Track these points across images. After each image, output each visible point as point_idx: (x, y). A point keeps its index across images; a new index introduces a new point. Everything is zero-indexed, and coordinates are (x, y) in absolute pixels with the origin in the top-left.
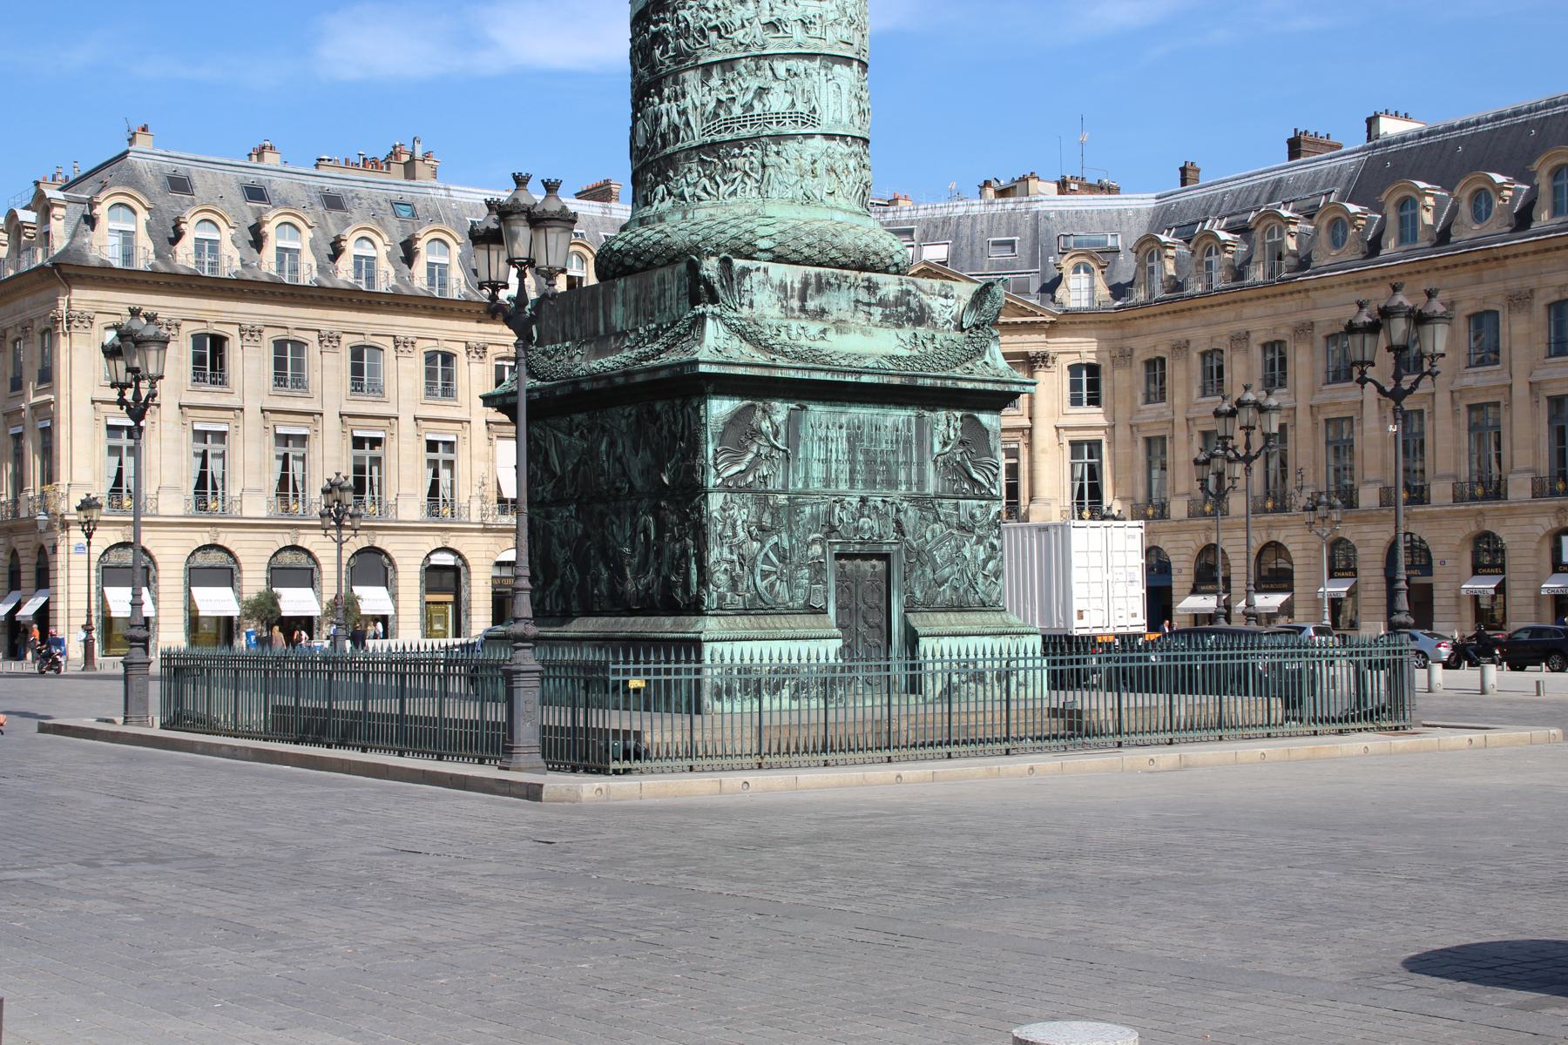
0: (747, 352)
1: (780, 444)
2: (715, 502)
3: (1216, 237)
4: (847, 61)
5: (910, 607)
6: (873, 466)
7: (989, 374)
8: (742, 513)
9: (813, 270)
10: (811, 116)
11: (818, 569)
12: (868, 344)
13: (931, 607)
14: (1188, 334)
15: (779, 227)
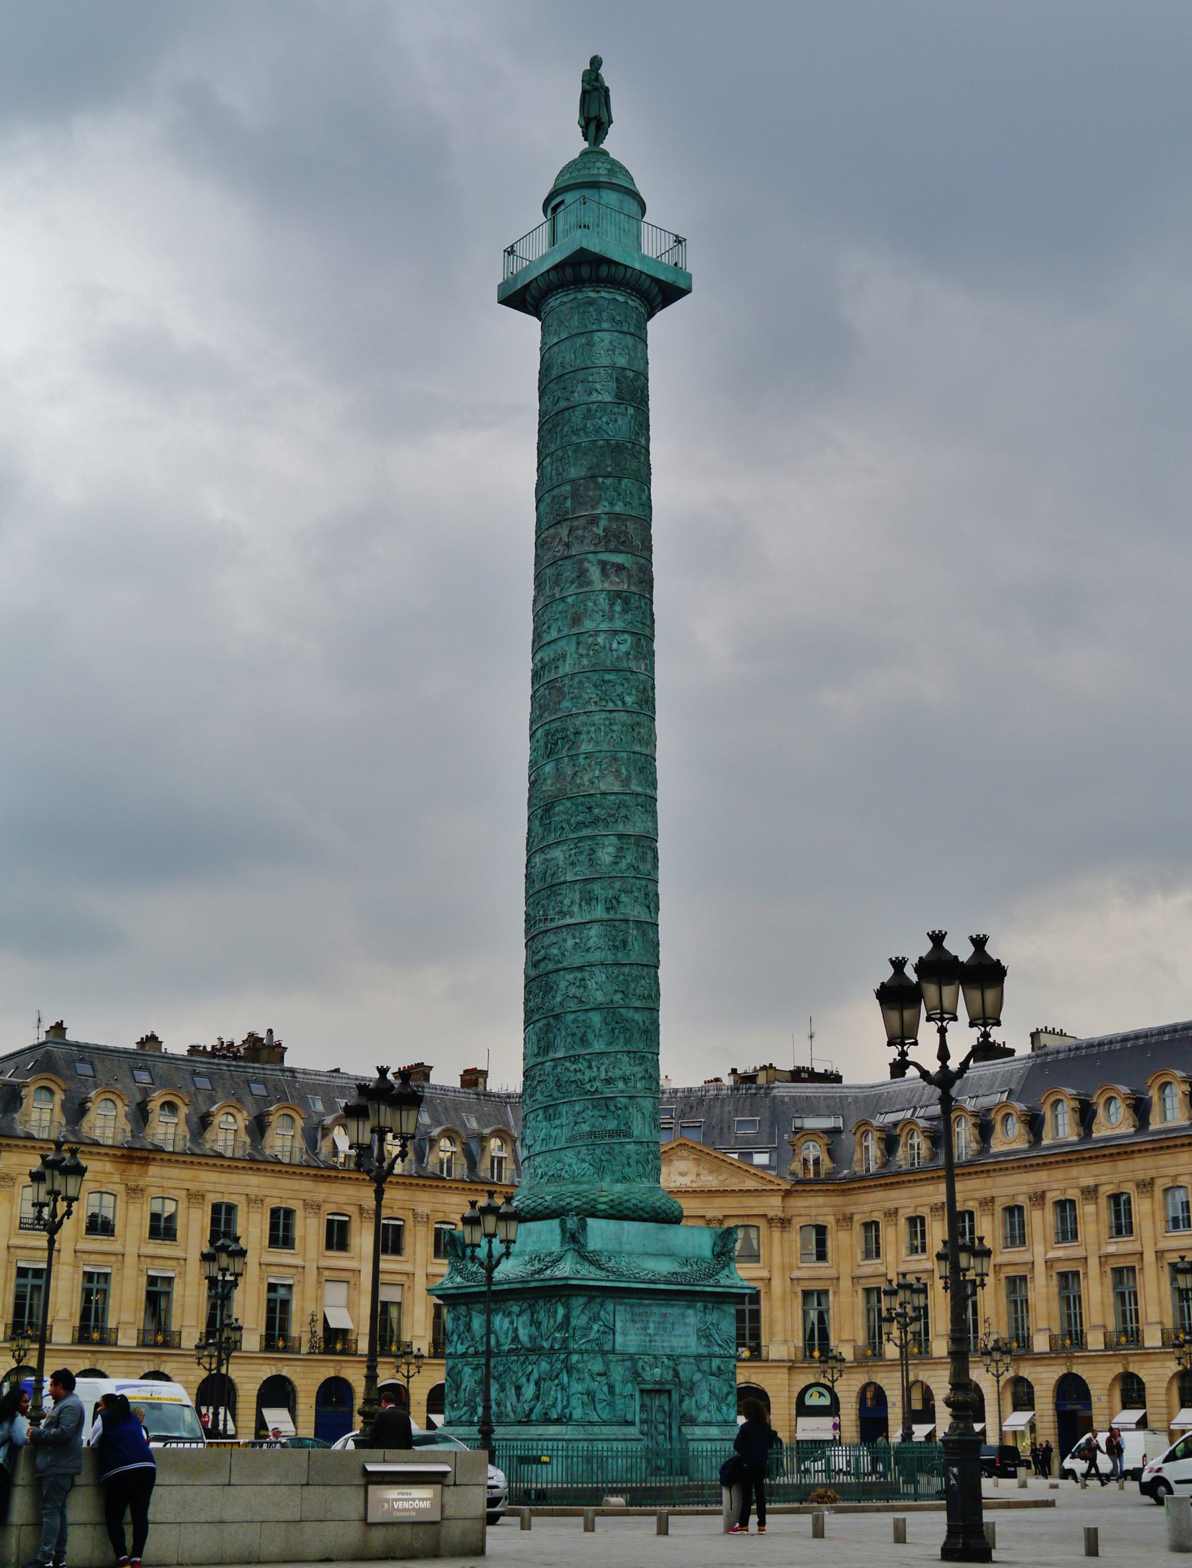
15: (611, 1197)
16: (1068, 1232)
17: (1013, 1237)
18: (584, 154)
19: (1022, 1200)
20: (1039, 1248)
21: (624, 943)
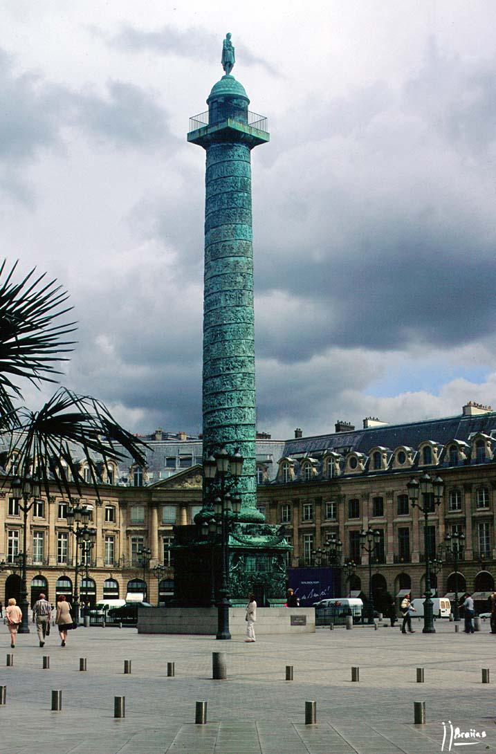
0: (237, 543)
1: (242, 562)
2: (231, 574)
3: (309, 461)
4: (252, 476)
5: (267, 597)
6: (261, 567)
7: (284, 546)
8: (236, 577)
9: (248, 524)
10: (246, 489)
11: (250, 590)
12: (261, 540)
13: (271, 597)
14: (300, 497)
16: (378, 511)
17: (353, 513)
18: (224, 78)
19: (358, 497)
20: (365, 519)
21: (244, 415)
